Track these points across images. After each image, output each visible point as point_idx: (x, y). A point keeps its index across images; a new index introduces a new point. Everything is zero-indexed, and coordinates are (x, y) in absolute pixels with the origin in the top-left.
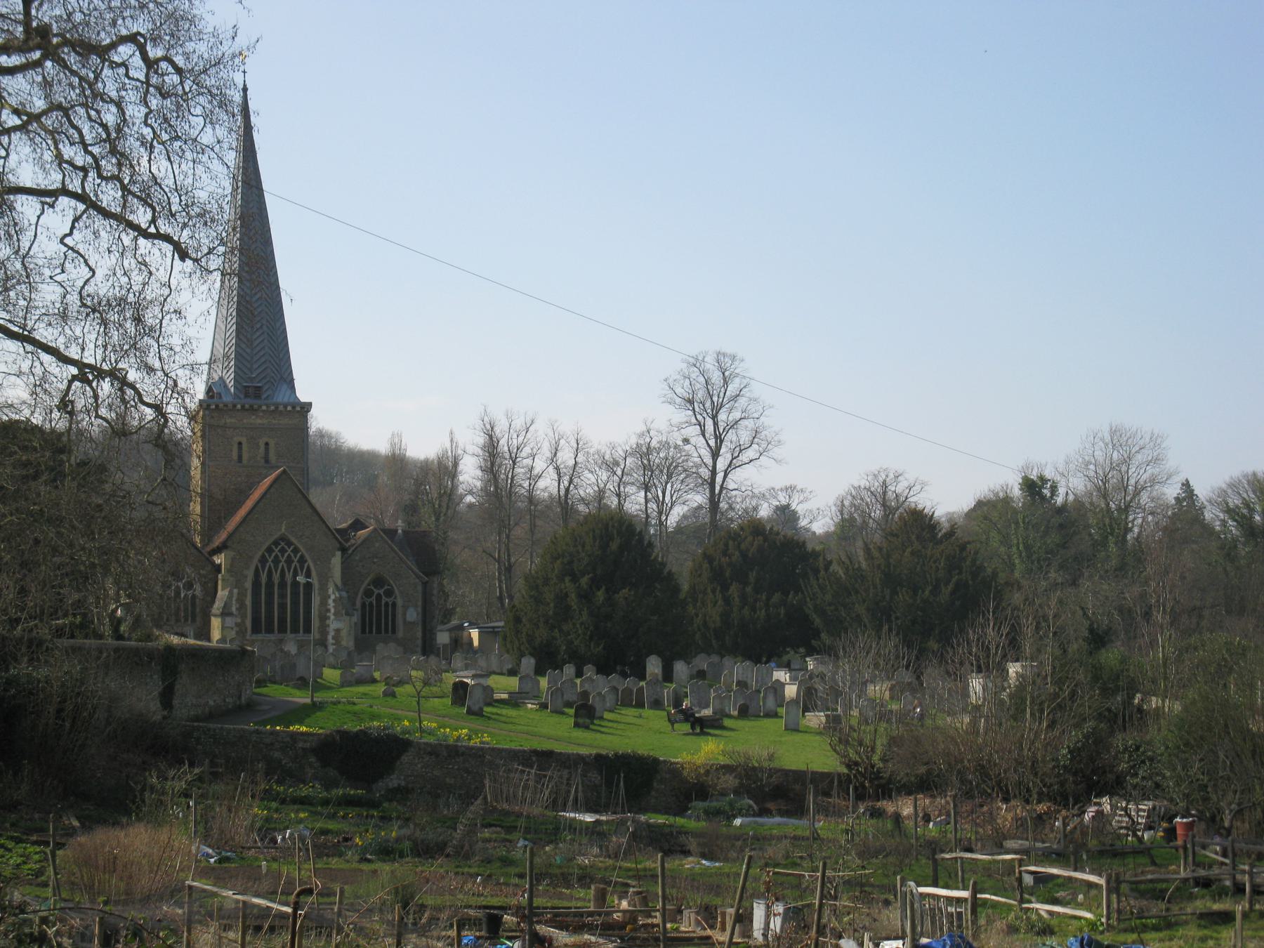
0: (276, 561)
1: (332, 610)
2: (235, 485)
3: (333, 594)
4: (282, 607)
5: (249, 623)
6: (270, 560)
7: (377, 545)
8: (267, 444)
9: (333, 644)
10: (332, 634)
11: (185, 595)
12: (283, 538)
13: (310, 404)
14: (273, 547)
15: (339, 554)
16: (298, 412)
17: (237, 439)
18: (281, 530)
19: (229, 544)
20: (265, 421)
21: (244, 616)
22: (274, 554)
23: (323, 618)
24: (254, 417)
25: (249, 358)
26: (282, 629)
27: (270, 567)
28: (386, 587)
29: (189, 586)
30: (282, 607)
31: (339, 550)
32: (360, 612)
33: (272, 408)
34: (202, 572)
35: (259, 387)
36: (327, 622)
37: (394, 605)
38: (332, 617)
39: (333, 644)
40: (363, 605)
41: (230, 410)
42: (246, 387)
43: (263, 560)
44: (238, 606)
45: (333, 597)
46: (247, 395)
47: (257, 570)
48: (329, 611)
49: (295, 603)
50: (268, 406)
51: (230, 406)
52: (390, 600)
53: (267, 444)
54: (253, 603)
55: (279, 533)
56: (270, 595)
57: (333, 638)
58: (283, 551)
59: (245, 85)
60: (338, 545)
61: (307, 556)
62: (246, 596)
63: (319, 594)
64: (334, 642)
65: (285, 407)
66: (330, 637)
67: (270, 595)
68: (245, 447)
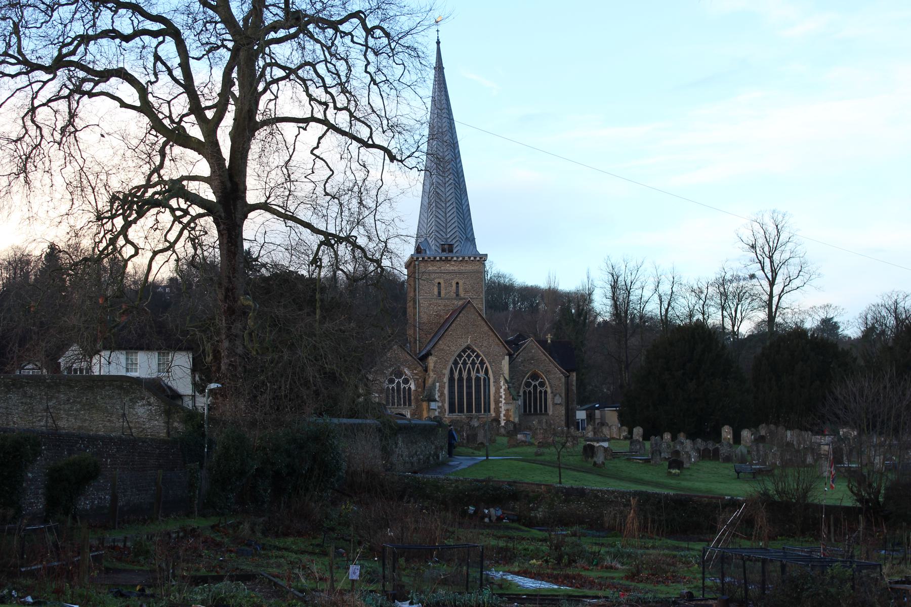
0: (465, 363)
1: (503, 397)
2: (436, 312)
3: (503, 386)
4: (469, 394)
5: (447, 406)
8: (457, 283)
9: (504, 420)
12: (468, 347)
13: (486, 255)
14: (462, 353)
15: (507, 358)
16: (478, 260)
17: (437, 281)
19: (433, 352)
20: (456, 268)
21: (443, 402)
23: (497, 402)
24: (448, 265)
25: (444, 225)
27: (460, 367)
29: (406, 381)
30: (469, 394)
32: (522, 398)
33: (461, 259)
34: (415, 372)
35: (451, 243)
36: (500, 405)
37: (546, 392)
39: (504, 420)
40: (525, 392)
41: (432, 261)
42: (442, 245)
43: (456, 363)
44: (439, 394)
45: (503, 387)
46: (443, 250)
47: (451, 369)
48: (501, 397)
50: (458, 258)
51: (432, 258)
52: (543, 390)
53: (457, 283)
54: (449, 392)
55: (466, 344)
56: (461, 387)
57: (504, 415)
58: (469, 356)
59: (438, 40)
60: (507, 352)
62: (445, 388)
64: (505, 418)
65: (469, 258)
66: (502, 415)
67: (461, 387)
68: (443, 285)
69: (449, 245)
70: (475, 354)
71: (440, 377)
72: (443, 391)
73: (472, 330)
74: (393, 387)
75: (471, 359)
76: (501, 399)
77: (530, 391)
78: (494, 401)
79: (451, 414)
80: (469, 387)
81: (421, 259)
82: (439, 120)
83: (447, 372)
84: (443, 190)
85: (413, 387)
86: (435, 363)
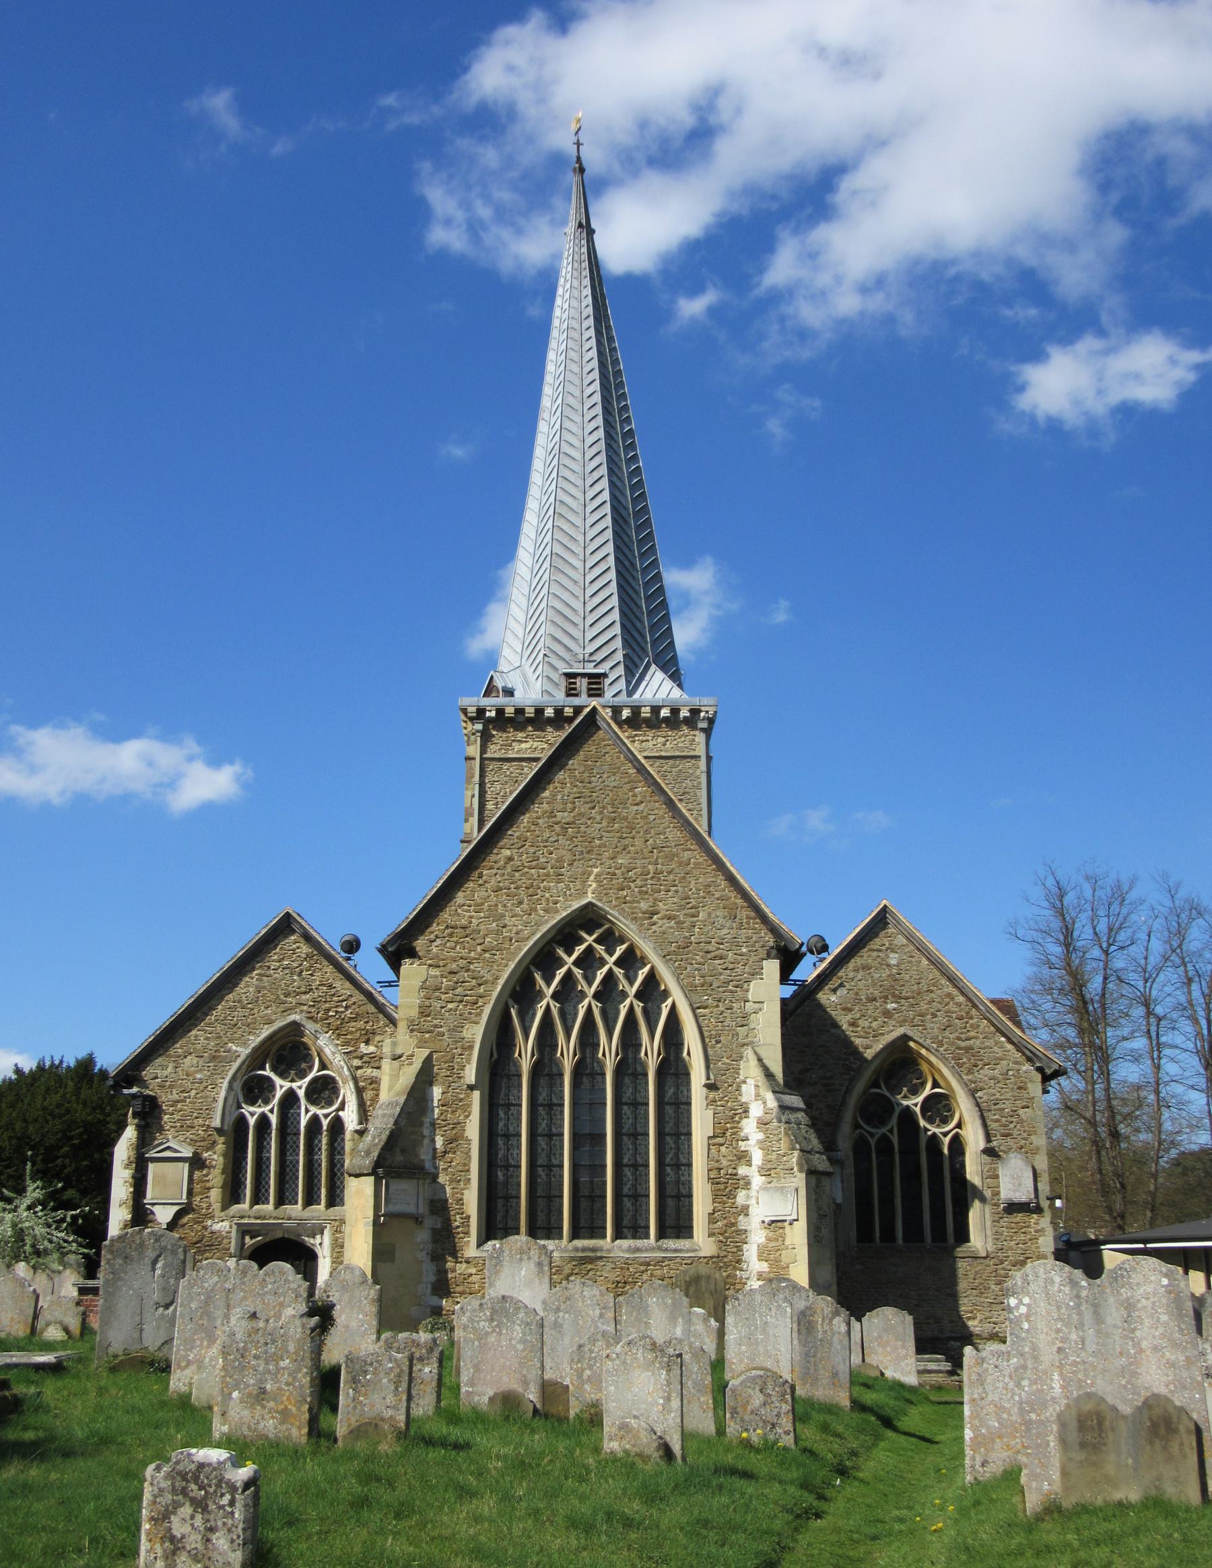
1: (757, 1157)
4: (587, 1139)
7: (893, 959)
10: (757, 1237)
11: (315, 1121)
12: (588, 918)
14: (561, 952)
15: (772, 967)
22: (560, 974)
26: (588, 1224)
28: (927, 1091)
30: (587, 1139)
31: (769, 956)
36: (741, 1197)
38: (757, 1181)
40: (860, 1147)
42: (569, 676)
46: (571, 692)
48: (743, 1157)
49: (630, 1135)
51: (530, 712)
55: (576, 905)
58: (588, 962)
60: (770, 940)
61: (668, 979)
64: (764, 1267)
66: (751, 1253)
67: (544, 1107)
69: (590, 676)
70: (620, 950)
74: (263, 1121)
76: (742, 1170)
77: (885, 1141)
80: (587, 1105)
81: (493, 714)
82: (571, 344)
83: (476, 1033)
84: (578, 521)
85: (350, 1118)
86: (429, 989)
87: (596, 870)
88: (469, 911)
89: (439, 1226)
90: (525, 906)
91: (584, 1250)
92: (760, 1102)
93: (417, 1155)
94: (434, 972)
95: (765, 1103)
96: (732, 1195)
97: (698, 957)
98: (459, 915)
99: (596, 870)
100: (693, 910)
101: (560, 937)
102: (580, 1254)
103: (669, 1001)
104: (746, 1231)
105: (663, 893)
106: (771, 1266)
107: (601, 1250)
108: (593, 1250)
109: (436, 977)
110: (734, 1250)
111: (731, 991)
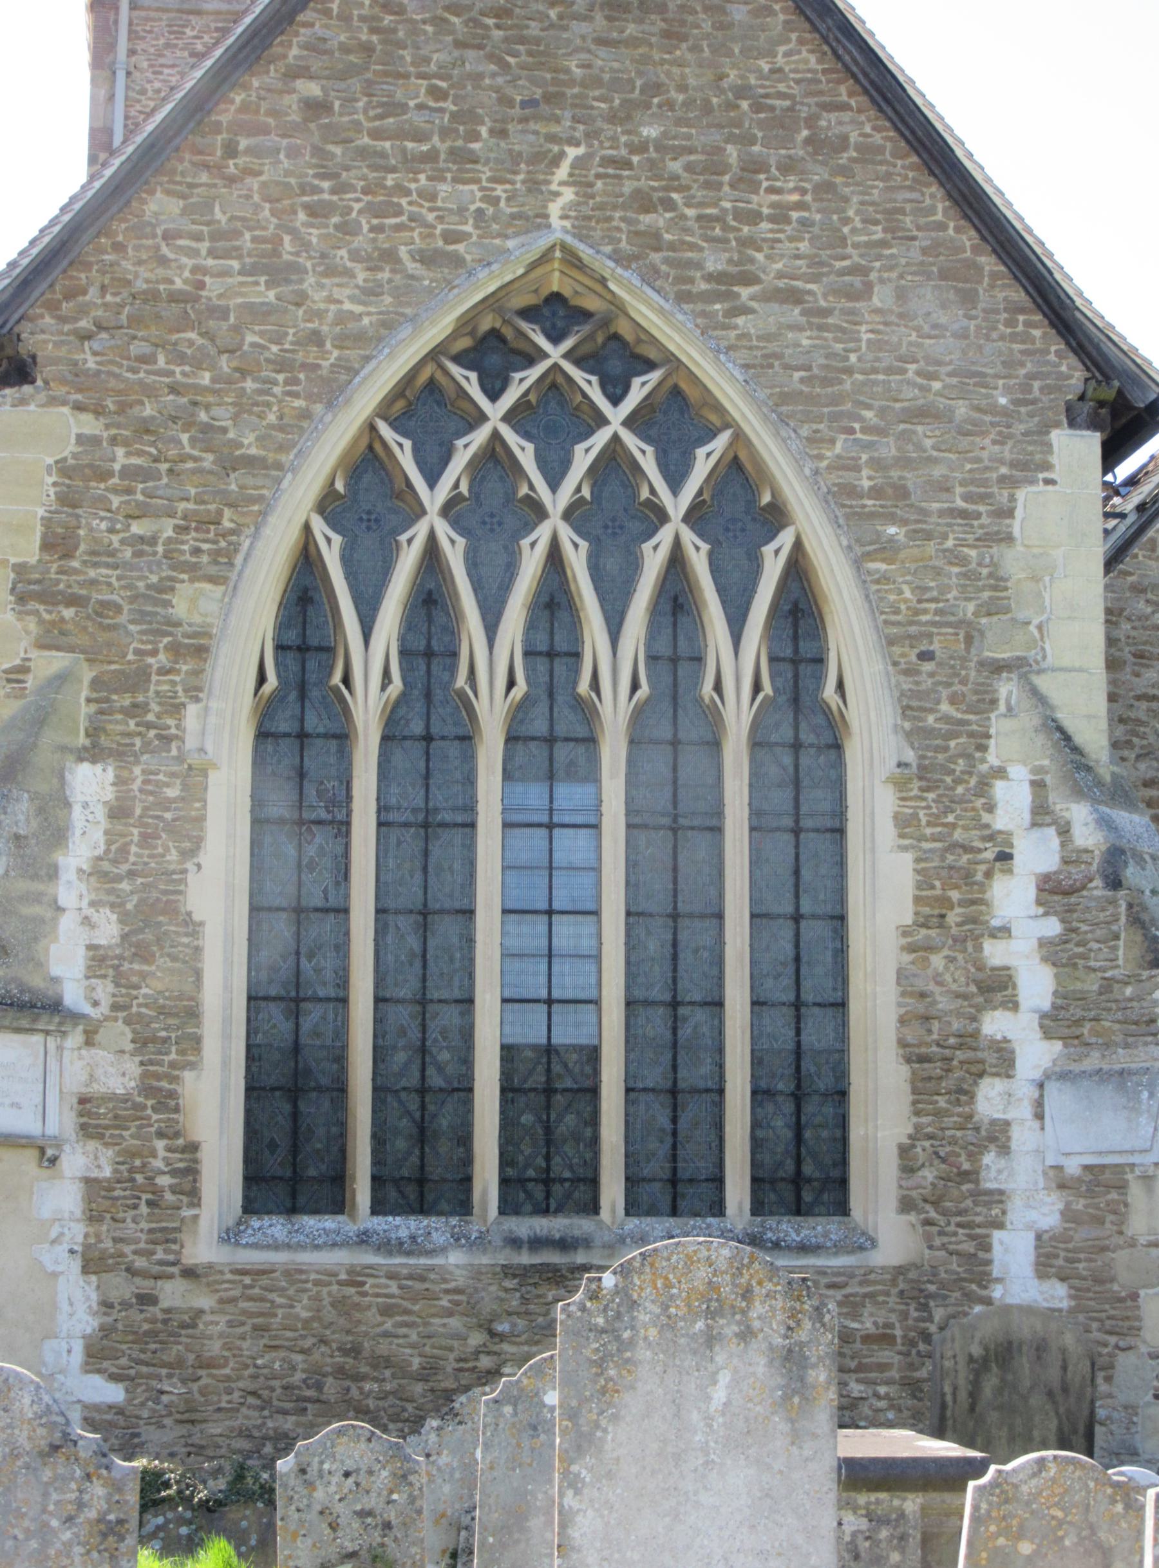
6: (433, 499)
18: (538, 221)
27: (432, 551)
44: (108, 930)
60: (1074, 375)
62: (193, 848)
63: (904, 823)
70: (638, 391)
71: (138, 679)
72: (175, 881)
73: (604, 59)
75: (583, 457)
76: (995, 1024)
78: (914, 1057)
79: (276, 1227)
87: (572, 152)
88: (195, 253)
89: (107, 1172)
90: (358, 242)
91: (537, 1243)
92: (1051, 831)
93: (40, 965)
94: (90, 425)
95: (1064, 831)
96: (964, 1094)
97: (868, 414)
98: (163, 261)
99: (572, 152)
100: (857, 281)
101: (464, 343)
102: (526, 1258)
103: (786, 539)
104: (1001, 1192)
105: (765, 225)
106: (1077, 1294)
107: (585, 1243)
108: (564, 1244)
109: (95, 441)
110: (969, 1247)
111: (964, 514)
